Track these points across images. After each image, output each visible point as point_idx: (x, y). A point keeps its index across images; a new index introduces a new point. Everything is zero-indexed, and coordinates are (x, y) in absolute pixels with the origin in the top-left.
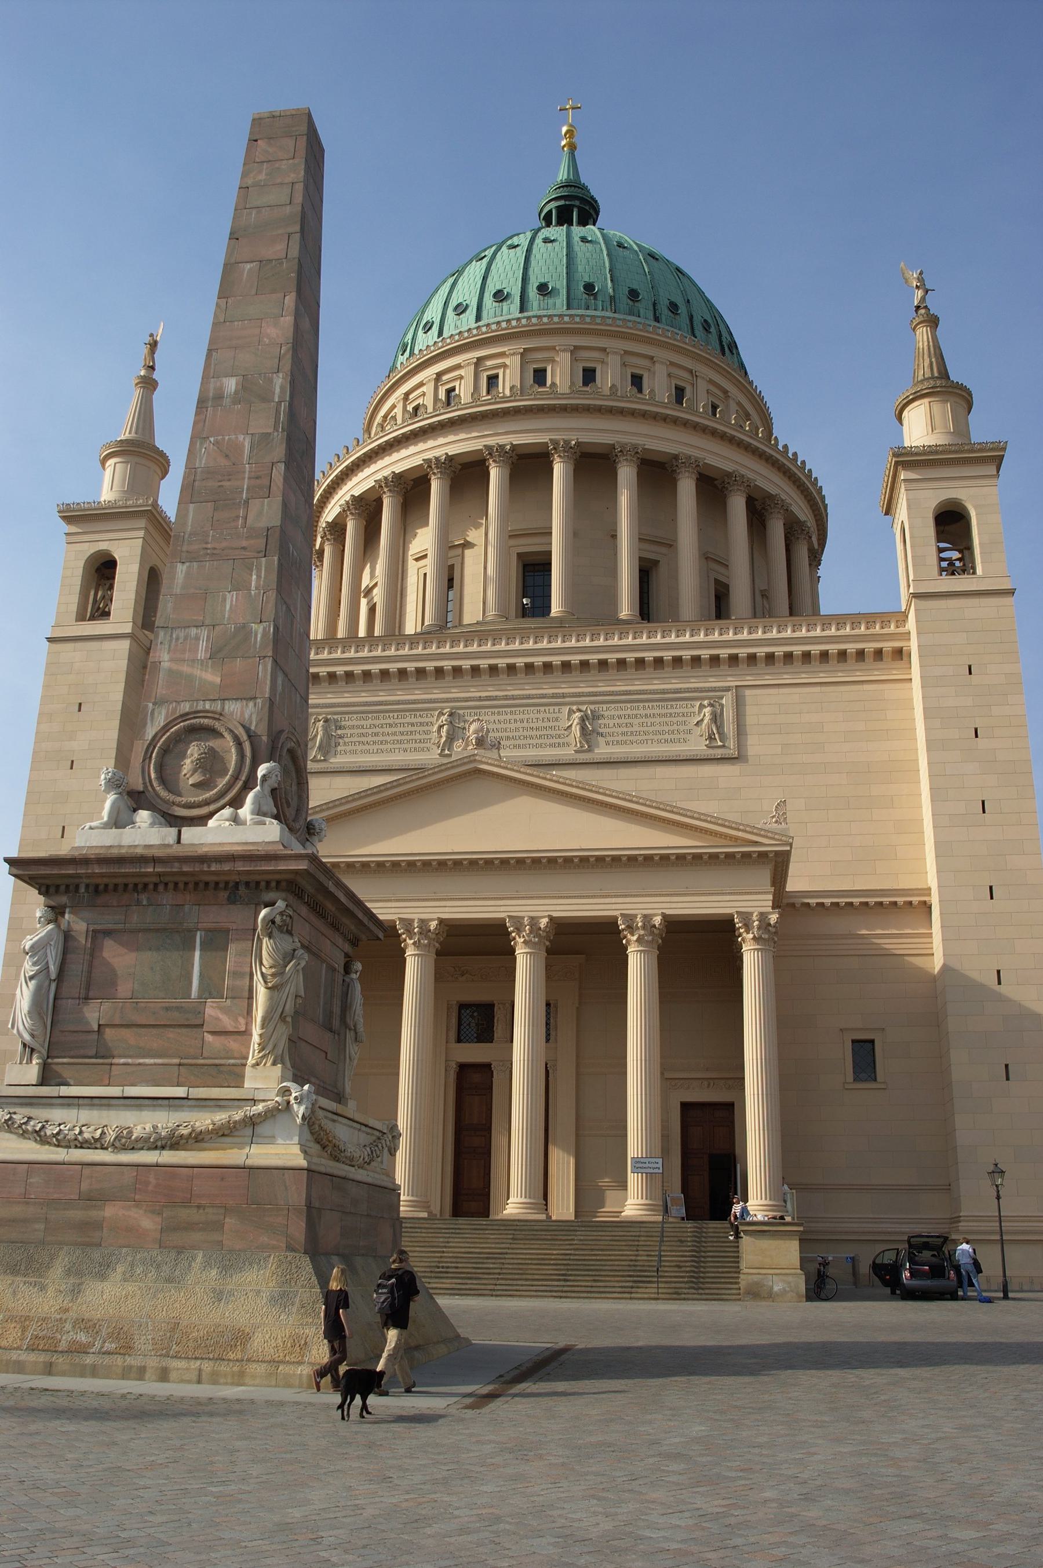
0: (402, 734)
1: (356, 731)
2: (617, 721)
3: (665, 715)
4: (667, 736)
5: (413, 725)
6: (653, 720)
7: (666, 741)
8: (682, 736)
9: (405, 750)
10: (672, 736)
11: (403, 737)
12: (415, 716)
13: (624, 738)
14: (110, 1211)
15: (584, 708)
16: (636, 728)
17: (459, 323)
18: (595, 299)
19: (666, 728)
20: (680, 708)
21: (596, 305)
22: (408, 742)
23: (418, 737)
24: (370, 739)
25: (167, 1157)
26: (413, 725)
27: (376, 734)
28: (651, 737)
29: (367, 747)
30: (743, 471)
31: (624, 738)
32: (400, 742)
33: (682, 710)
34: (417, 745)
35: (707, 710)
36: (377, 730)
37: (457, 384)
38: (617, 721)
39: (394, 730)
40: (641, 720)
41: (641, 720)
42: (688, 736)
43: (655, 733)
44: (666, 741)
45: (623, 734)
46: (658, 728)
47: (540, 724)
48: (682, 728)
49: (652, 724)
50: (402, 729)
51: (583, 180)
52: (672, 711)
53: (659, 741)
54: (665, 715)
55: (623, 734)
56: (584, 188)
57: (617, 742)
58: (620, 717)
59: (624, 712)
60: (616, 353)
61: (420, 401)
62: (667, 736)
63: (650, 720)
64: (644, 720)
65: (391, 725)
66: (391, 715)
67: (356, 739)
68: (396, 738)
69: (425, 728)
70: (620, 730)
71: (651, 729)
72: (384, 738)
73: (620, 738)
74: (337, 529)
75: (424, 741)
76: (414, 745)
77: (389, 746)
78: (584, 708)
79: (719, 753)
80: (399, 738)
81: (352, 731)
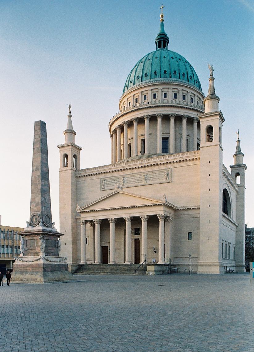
14: (28, 268)
16: (154, 178)
18: (157, 75)
25: (32, 263)
30: (185, 114)
35: (166, 173)
47: (138, 178)
51: (166, 32)
56: (165, 35)
61: (130, 101)
79: (168, 181)
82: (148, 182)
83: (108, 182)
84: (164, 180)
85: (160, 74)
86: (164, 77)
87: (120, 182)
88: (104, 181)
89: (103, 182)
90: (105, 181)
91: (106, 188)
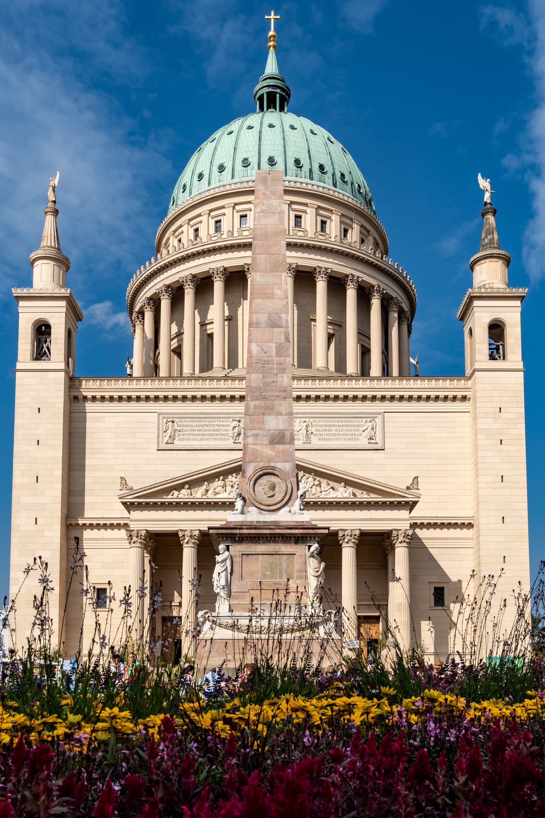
0: (213, 430)
1: (189, 428)
2: (324, 428)
3: (348, 426)
4: (349, 437)
5: (219, 426)
6: (342, 428)
7: (349, 439)
8: (357, 437)
9: (216, 439)
10: (352, 437)
11: (214, 433)
12: (220, 421)
13: (328, 437)
15: (307, 420)
16: (333, 432)
17: (221, 178)
18: (301, 170)
19: (349, 433)
20: (356, 422)
21: (301, 174)
22: (217, 435)
23: (222, 432)
24: (196, 432)
26: (219, 426)
27: (200, 430)
28: (341, 437)
29: (195, 437)
31: (328, 437)
32: (213, 435)
33: (357, 424)
34: (222, 437)
36: (200, 428)
37: (221, 218)
38: (324, 428)
39: (210, 428)
40: (336, 428)
41: (336, 428)
42: (359, 437)
43: (345, 435)
44: (349, 439)
45: (327, 435)
46: (344, 432)
48: (357, 433)
49: (342, 430)
50: (213, 428)
52: (352, 424)
53: (345, 439)
54: (348, 426)
55: (327, 435)
57: (324, 439)
58: (325, 426)
59: (328, 424)
60: (312, 207)
62: (349, 437)
63: (340, 428)
64: (337, 428)
65: (207, 426)
66: (207, 420)
67: (189, 432)
68: (210, 432)
69: (226, 428)
70: (326, 433)
71: (341, 433)
72: (204, 433)
73: (326, 437)
74: (155, 302)
75: (225, 435)
76: (220, 437)
77: (207, 437)
78: (307, 420)
80: (212, 433)
81: (187, 428)
82: (315, 442)
83: (187, 426)
84: (363, 442)
85: (311, 171)
86: (320, 181)
87: (226, 430)
88: (173, 422)
89: (170, 423)
90: (175, 424)
91: (178, 443)
